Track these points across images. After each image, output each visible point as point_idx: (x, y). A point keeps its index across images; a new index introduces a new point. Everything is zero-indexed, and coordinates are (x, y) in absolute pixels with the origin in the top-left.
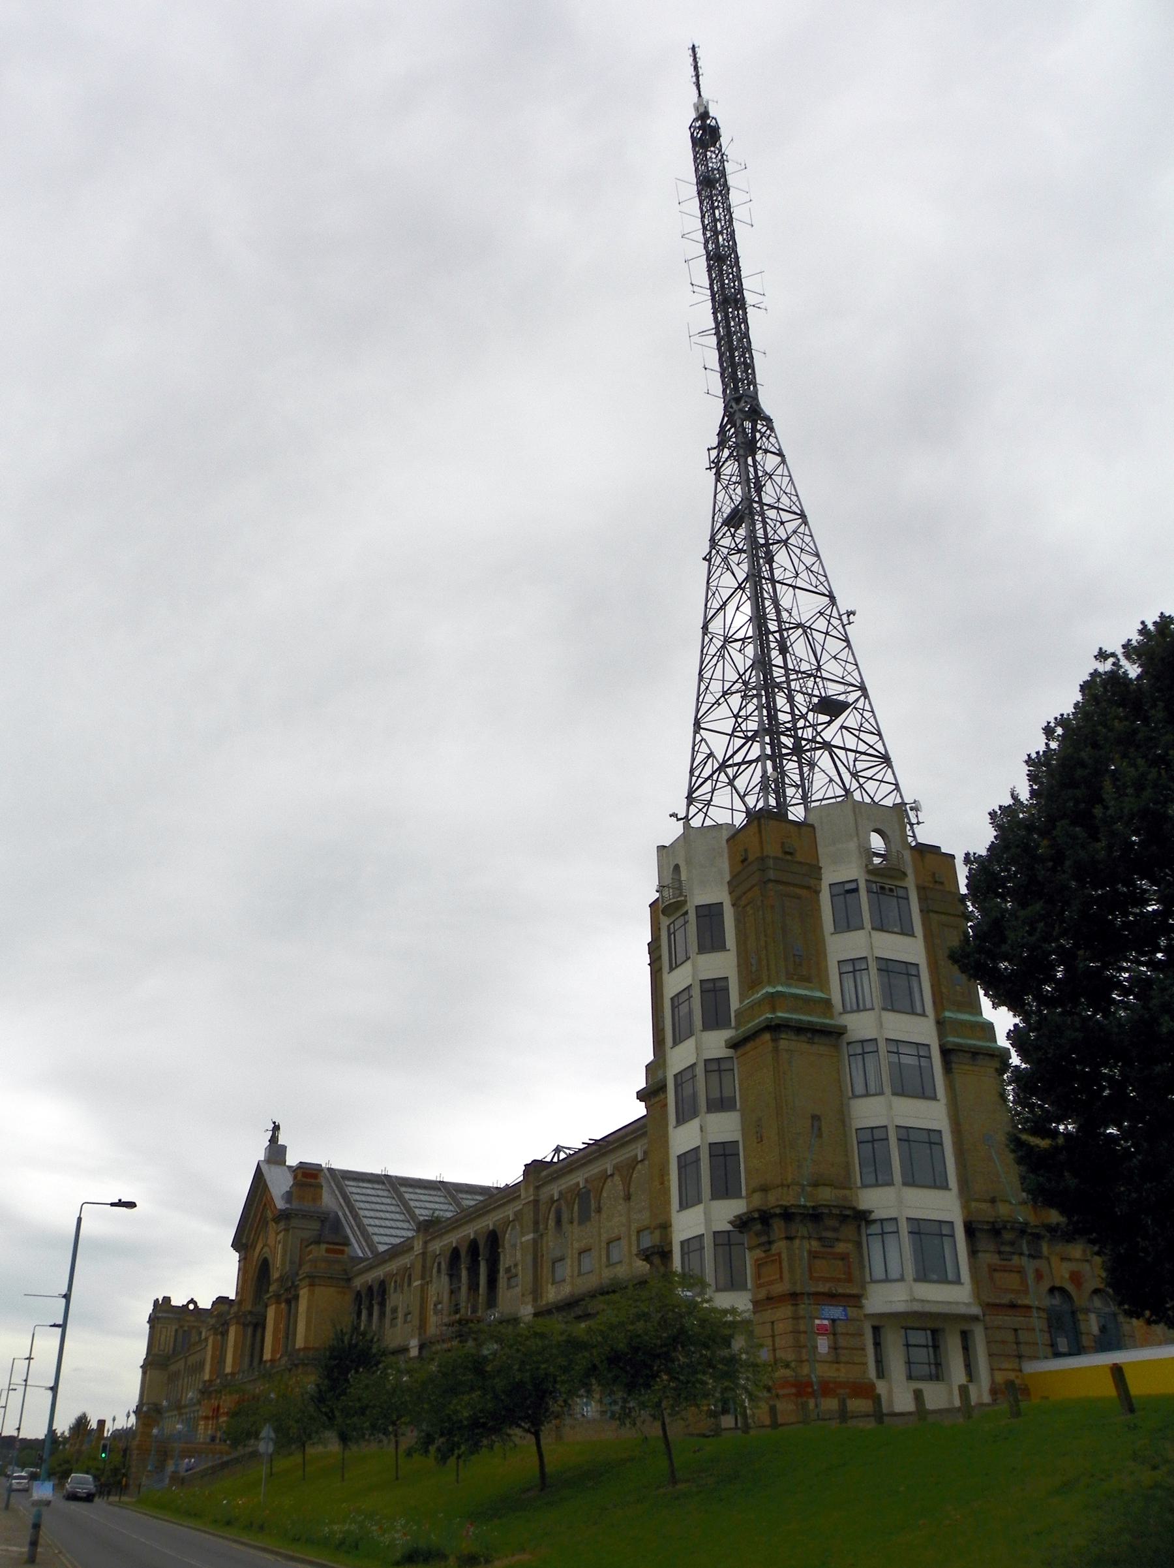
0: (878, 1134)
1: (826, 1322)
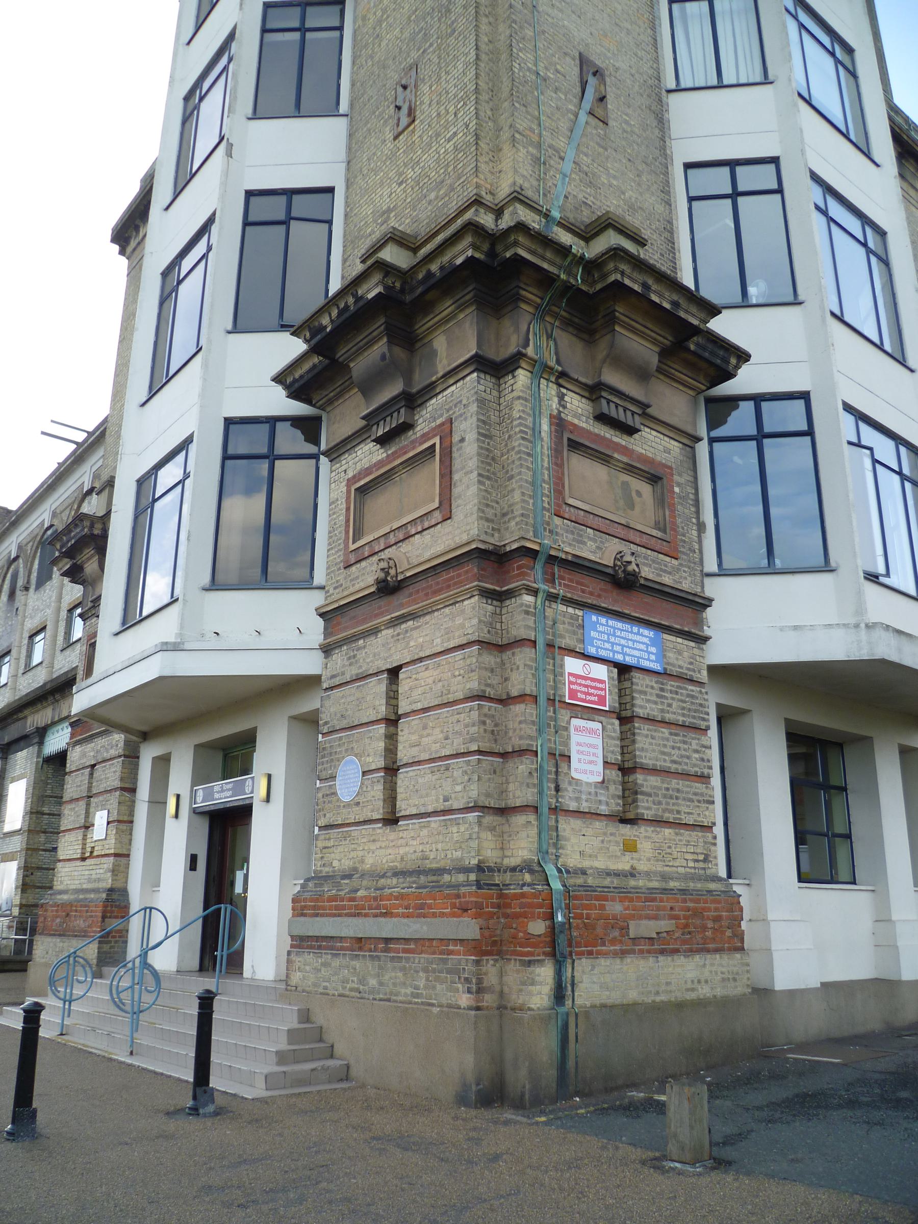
1: (600, 672)
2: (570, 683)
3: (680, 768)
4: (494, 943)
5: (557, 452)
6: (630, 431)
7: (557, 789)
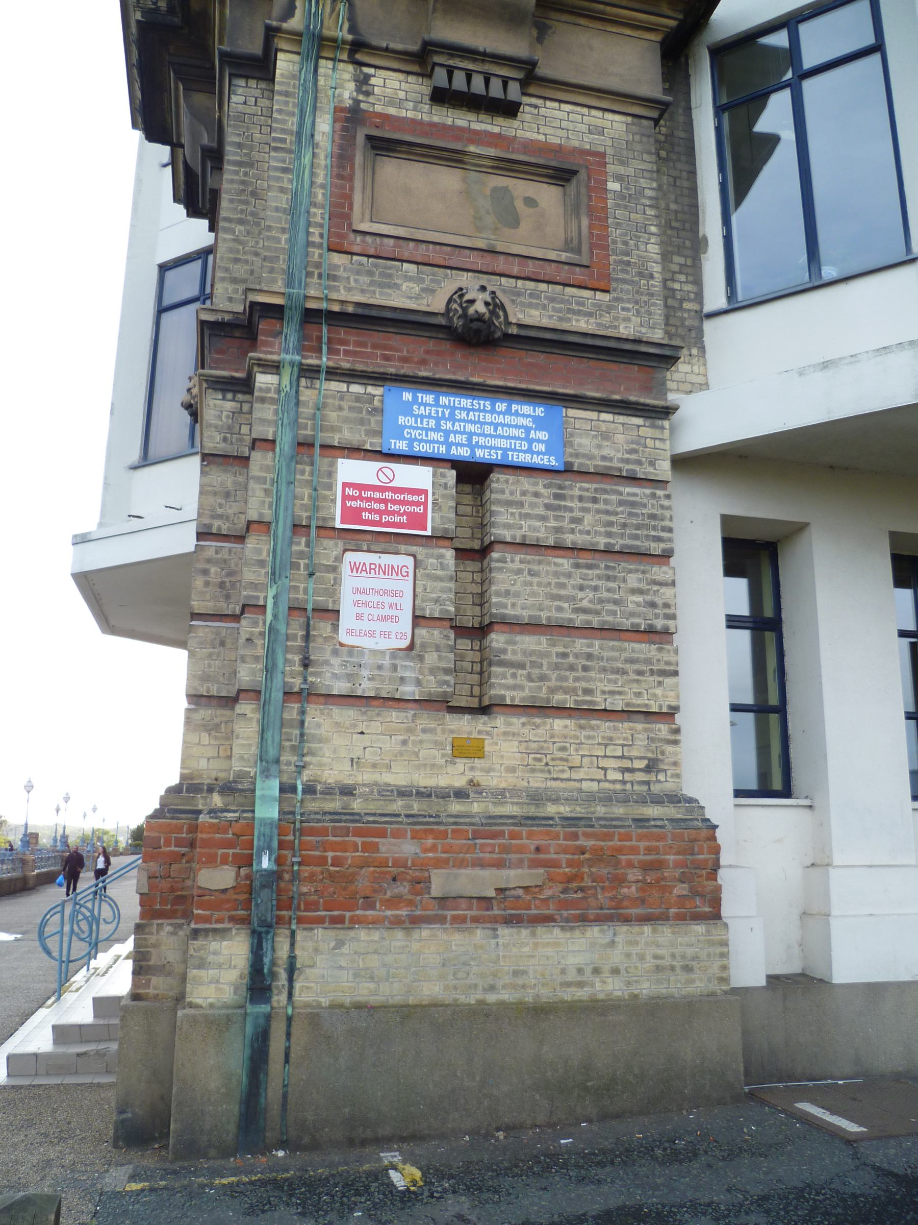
1: (419, 477)
2: (345, 498)
3: (596, 621)
4: (181, 899)
5: (342, 158)
6: (510, 110)
7: (306, 663)
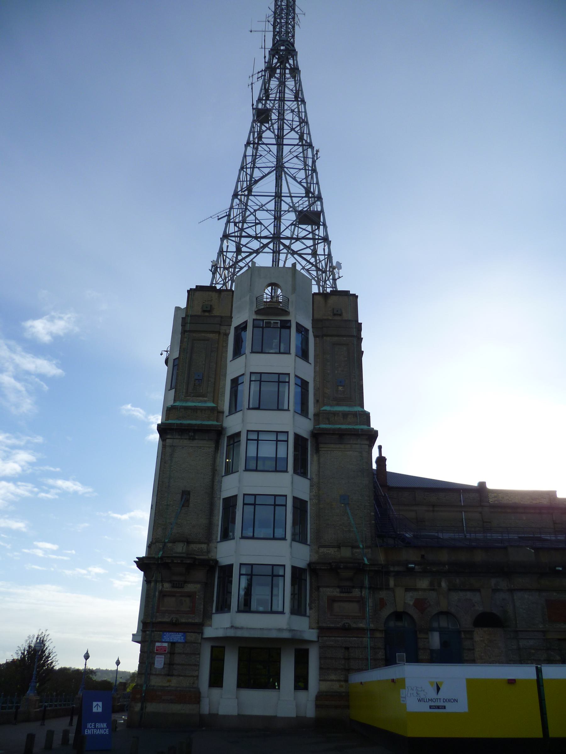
0: (279, 501)
1: (166, 645)
